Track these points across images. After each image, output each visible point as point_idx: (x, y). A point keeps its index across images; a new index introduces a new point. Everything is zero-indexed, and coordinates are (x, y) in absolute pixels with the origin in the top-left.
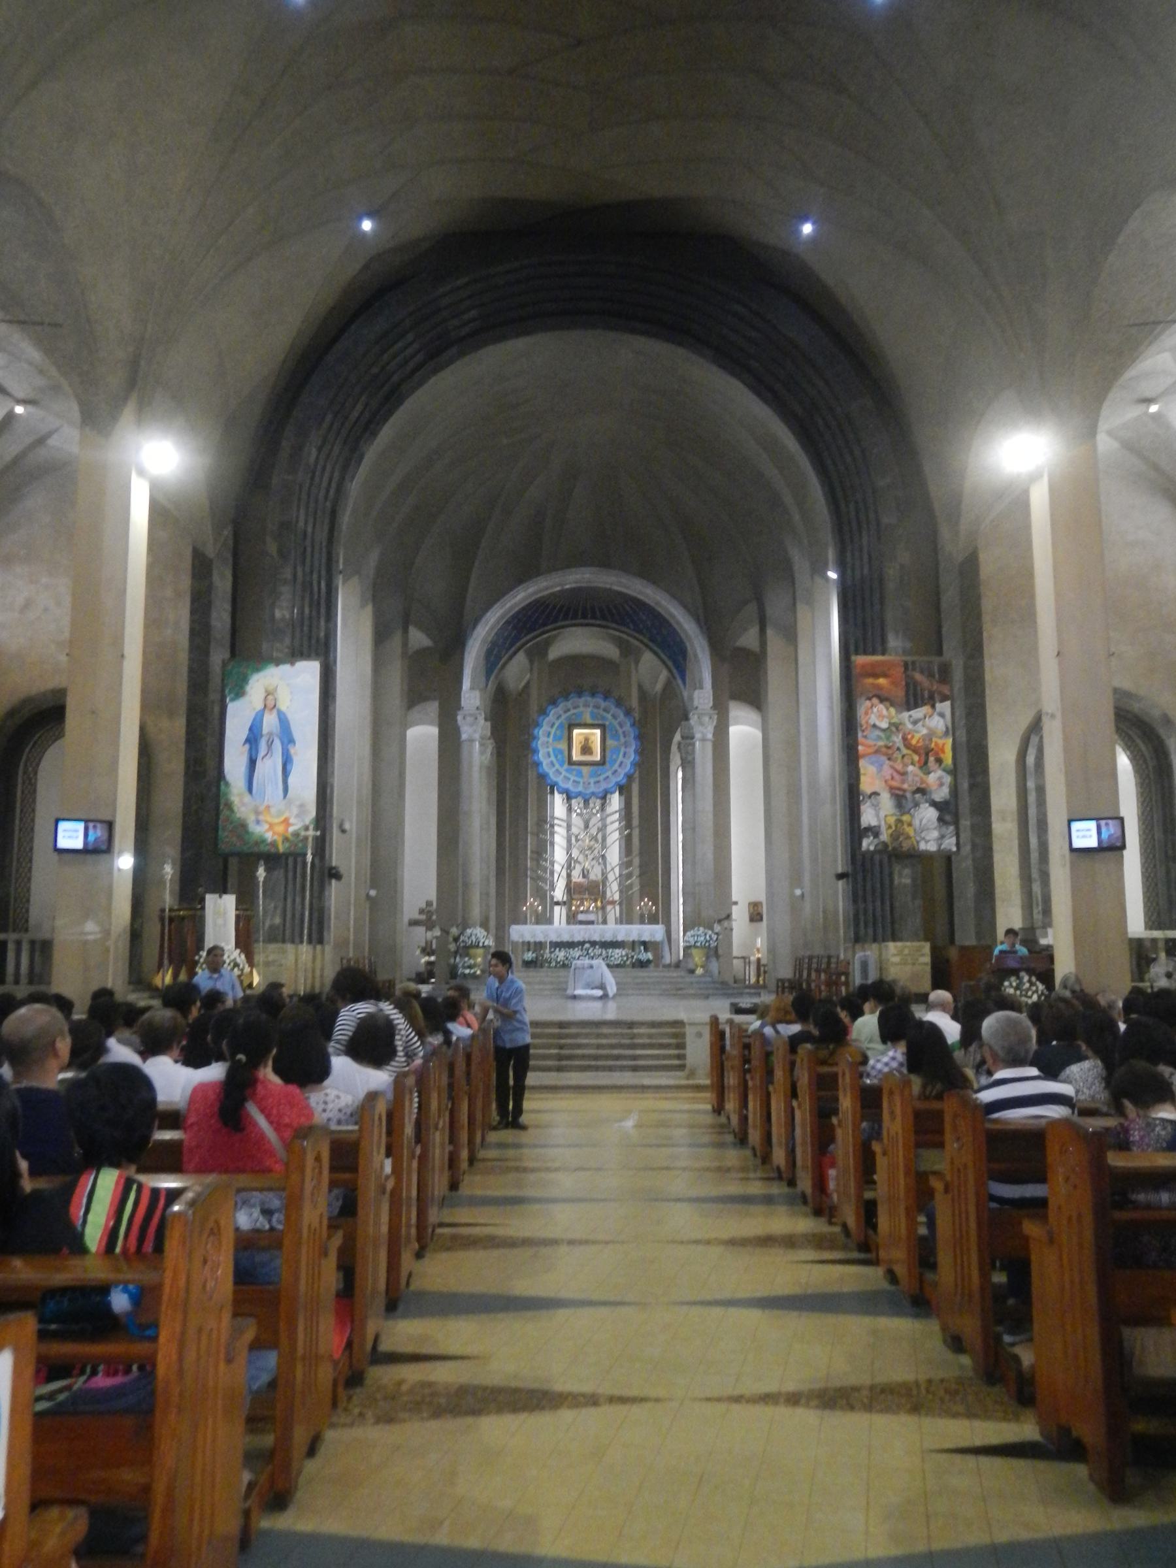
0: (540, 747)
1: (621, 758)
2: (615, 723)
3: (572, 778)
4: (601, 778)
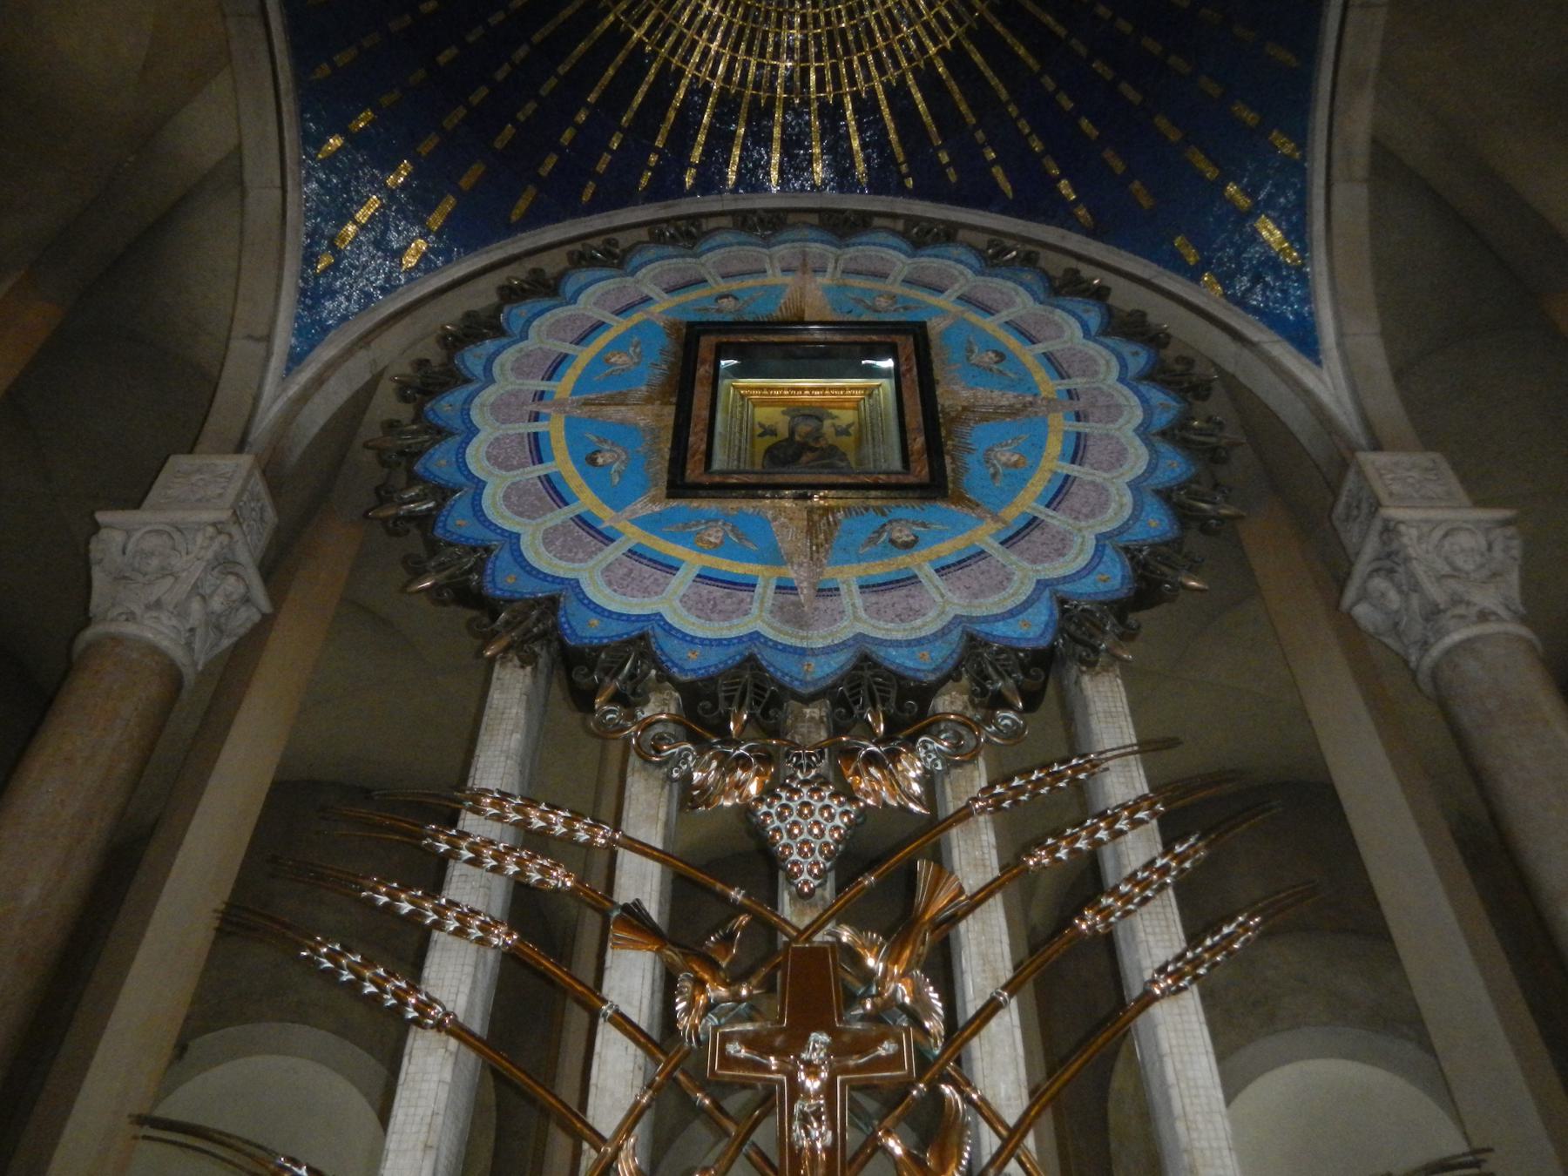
0: (476, 417)
1: (1053, 460)
2: (990, 324)
3: (692, 561)
4: (920, 562)
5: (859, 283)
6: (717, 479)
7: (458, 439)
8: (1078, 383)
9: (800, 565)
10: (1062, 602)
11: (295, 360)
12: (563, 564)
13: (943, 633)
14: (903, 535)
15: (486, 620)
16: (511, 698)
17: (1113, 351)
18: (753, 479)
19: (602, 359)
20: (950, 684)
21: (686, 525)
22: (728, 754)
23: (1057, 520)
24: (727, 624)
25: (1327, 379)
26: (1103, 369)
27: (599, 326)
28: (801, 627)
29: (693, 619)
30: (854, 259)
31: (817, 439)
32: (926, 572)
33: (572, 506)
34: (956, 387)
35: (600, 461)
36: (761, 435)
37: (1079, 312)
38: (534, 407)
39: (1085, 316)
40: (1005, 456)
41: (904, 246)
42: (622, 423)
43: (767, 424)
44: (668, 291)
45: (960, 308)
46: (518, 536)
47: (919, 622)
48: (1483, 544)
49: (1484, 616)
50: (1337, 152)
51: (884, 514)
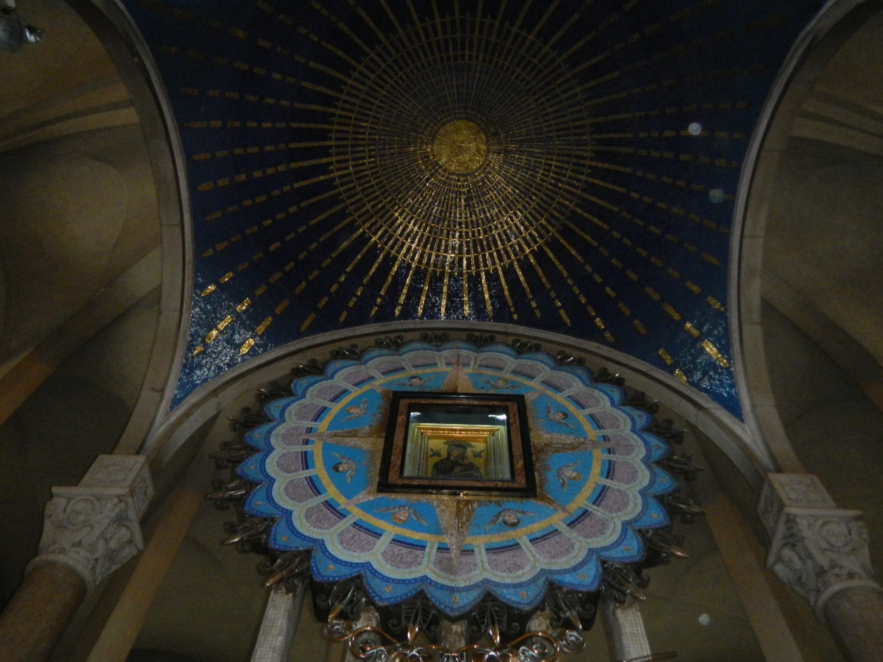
0: (273, 441)
1: (596, 476)
2: (559, 397)
3: (390, 530)
4: (521, 535)
5: (489, 372)
6: (406, 482)
7: (262, 454)
8: (609, 432)
9: (452, 535)
10: (604, 562)
11: (176, 402)
12: (316, 530)
13: (534, 580)
14: (513, 520)
15: (269, 563)
16: (279, 611)
17: (628, 414)
18: (426, 482)
19: (345, 410)
20: (539, 613)
21: (388, 509)
22: (406, 655)
23: (599, 512)
24: (408, 570)
25: (747, 429)
26: (622, 424)
27: (345, 392)
28: (451, 574)
29: (389, 567)
30: (485, 359)
31: (463, 459)
32: (524, 542)
33: (323, 495)
34: (541, 433)
35: (341, 469)
36: (432, 456)
37: (609, 392)
38: (306, 437)
39: (611, 394)
40: (569, 473)
41: (513, 353)
42: (355, 447)
43: (435, 449)
44: (383, 374)
45: (542, 388)
46: (291, 512)
47: (520, 572)
48: (846, 531)
49: (851, 575)
50: (743, 309)
51: (500, 505)
